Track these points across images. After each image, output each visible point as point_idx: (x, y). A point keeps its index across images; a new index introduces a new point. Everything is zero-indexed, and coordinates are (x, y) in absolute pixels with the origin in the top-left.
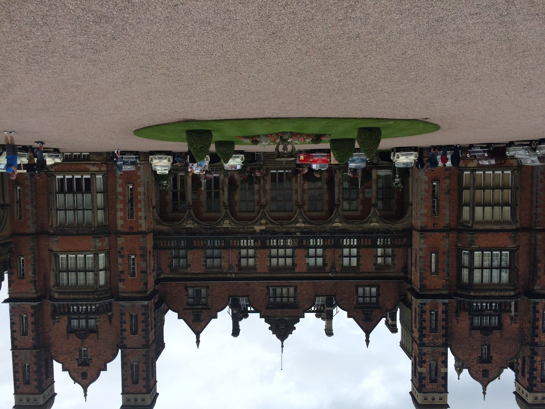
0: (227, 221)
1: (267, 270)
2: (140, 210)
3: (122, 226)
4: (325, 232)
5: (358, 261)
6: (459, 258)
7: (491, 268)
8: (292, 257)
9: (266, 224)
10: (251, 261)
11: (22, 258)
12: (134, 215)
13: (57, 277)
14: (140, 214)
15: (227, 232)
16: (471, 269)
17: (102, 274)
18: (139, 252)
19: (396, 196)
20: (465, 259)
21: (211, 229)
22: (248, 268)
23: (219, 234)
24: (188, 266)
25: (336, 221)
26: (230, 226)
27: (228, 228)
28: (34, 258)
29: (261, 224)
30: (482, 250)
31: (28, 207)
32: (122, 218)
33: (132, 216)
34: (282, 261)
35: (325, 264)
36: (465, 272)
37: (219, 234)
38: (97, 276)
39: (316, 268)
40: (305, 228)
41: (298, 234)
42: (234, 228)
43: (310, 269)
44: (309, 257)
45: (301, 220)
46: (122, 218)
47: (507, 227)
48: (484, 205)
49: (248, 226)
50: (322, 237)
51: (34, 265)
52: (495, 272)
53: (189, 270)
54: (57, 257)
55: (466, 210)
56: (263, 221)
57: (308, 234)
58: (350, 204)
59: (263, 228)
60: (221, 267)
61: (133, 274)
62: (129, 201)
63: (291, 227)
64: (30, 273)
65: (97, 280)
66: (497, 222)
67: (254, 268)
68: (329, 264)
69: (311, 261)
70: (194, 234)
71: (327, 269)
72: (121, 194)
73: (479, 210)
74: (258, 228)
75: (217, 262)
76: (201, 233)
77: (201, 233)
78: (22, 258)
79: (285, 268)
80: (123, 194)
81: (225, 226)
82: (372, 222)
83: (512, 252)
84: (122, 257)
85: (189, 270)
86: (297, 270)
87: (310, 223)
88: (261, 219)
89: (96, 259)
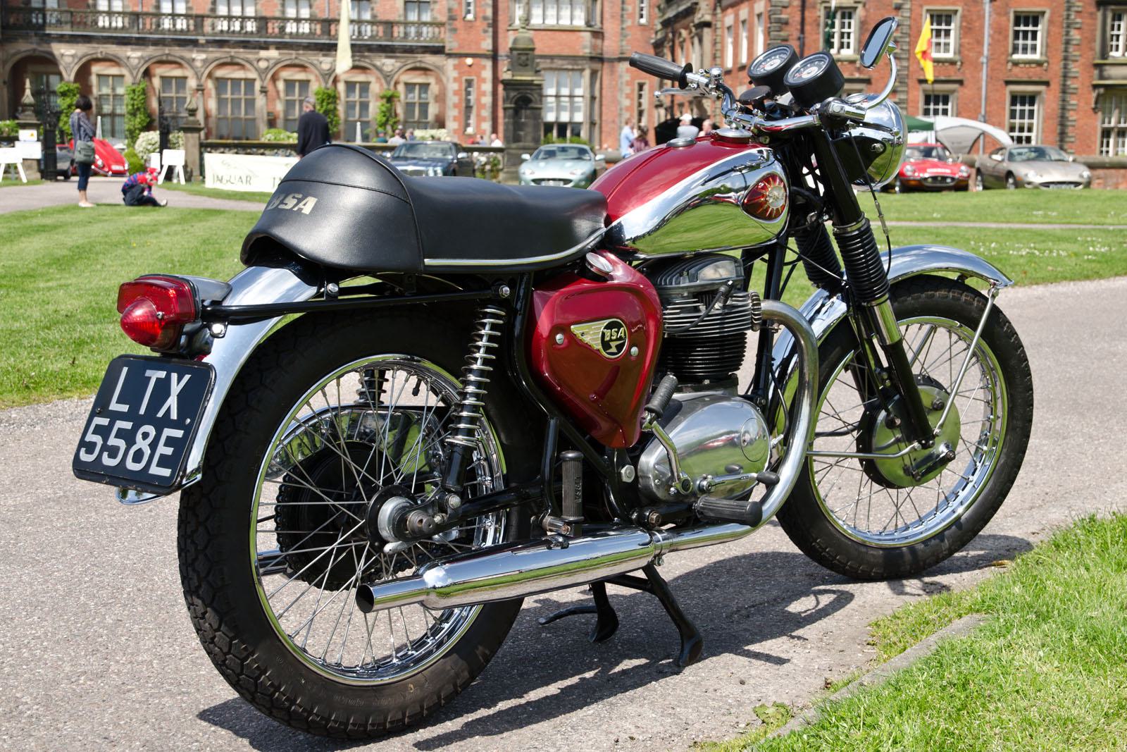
2: (456, 93)
3: (484, 67)
9: (259, 60)
11: (643, 21)
12: (464, 85)
14: (455, 86)
25: (136, 61)
26: (322, 59)
27: (324, 55)
28: (622, 22)
29: (267, 60)
31: (626, 103)
32: (484, 81)
33: (469, 83)
40: (191, 51)
42: (315, 55)
45: (198, 64)
46: (484, 81)
49: (288, 57)
50: (163, 32)
51: (623, 9)
54: (588, 24)
56: (263, 65)
59: (263, 54)
62: (471, 107)
72: (484, 119)
78: (643, 21)
80: (480, 119)
82: (73, 56)
84: (485, 18)
87: (182, 58)
88: (268, 69)
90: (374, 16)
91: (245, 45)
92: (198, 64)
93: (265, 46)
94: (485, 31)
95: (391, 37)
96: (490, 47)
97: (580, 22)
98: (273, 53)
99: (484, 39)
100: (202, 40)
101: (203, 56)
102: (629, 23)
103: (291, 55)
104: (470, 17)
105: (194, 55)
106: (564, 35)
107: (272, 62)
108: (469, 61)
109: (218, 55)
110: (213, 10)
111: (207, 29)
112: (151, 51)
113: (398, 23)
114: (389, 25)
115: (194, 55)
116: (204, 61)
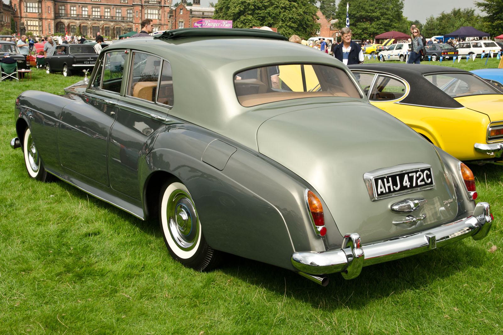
0: (112, 25)
1: (101, 7)
4: (82, 20)
5: (71, 8)
6: (42, 11)
7: (32, 7)
8: (93, 11)
10: (106, 10)
13: (158, 12)
16: (38, 7)
17: (146, 13)
18: (135, 18)
19: (59, 29)
20: (40, 10)
22: (108, 8)
23: (114, 21)
24: (127, 10)
30: (35, 13)
33: (137, 29)
34: (96, 10)
35: (82, 8)
36: (40, 6)
37: (114, 21)
38: (147, 12)
39: (85, 7)
41: (90, 19)
43: (86, 7)
44: (87, 11)
47: (29, 19)
48: (36, 26)
52: (31, 6)
53: (127, 9)
54: (158, 19)
55: (41, 25)
56: (101, 24)
57: (87, 19)
58: (74, 27)
59: (101, 22)
60: (116, 9)
61: (137, 12)
63: (92, 22)
64: (166, 14)
65: (147, 11)
66: (31, 20)
67: (105, 8)
68: (80, 8)
69: (86, 9)
70: (122, 22)
71: (81, 6)
73: (37, 24)
74: (102, 22)
75: (117, 11)
76: (120, 22)
77: (120, 22)
79: (95, 8)
81: (112, 23)
83: (27, 12)
85: (127, 9)
86: (91, 7)
88: (102, 25)
89: (147, 17)
91: (98, 20)
93: (101, 21)
97: (157, 18)
102: (166, 19)
105: (89, 22)
108: (137, 25)
110: (92, 14)
111: (91, 17)
112: (81, 21)
113: (125, 17)
114: (124, 17)
115: (89, 22)
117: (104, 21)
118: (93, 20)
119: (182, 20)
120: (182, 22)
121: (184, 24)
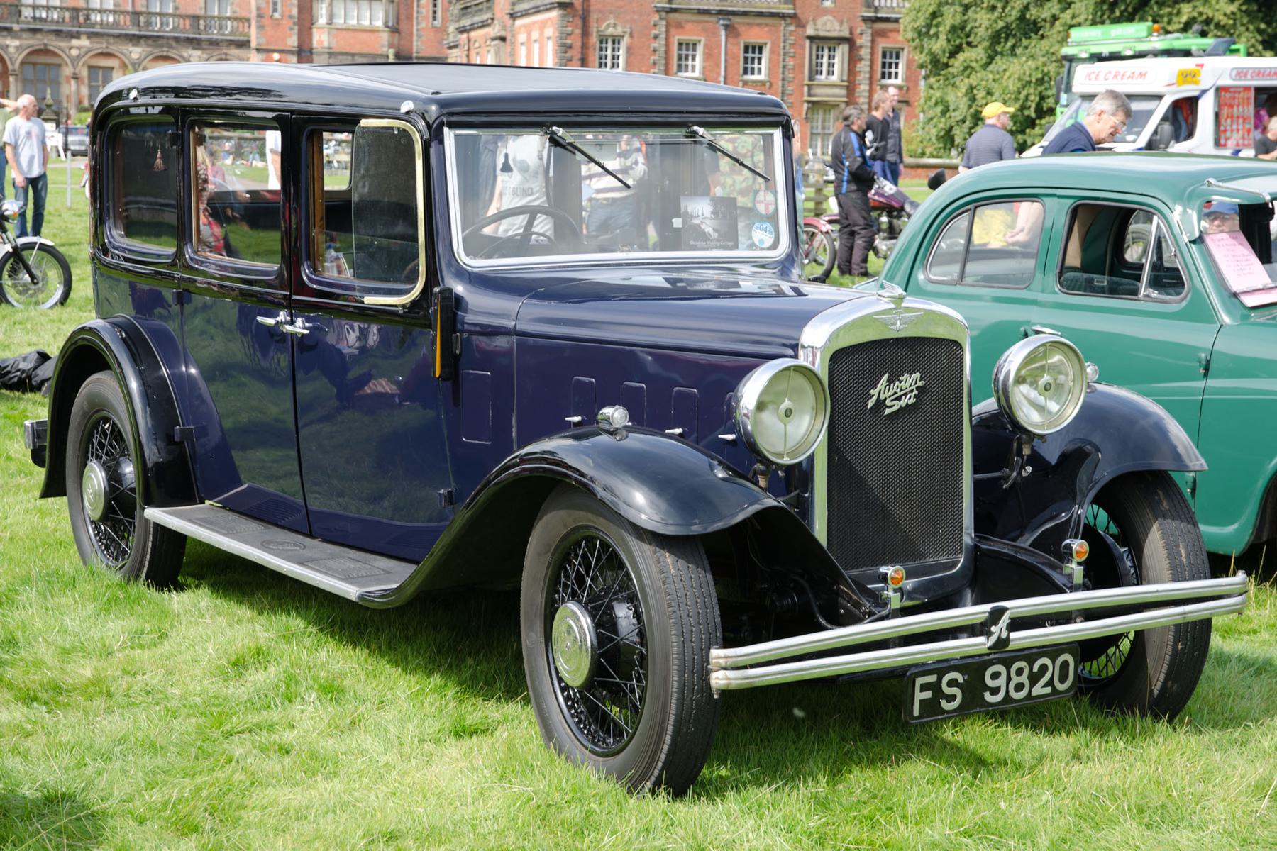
0: (134, 56)
15: (135, 39)
18: (266, 21)
21: (162, 46)
26: (131, 48)
29: (79, 48)
40: (4, 37)
56: (74, 52)
59: (75, 42)
76: (177, 39)
81: (138, 49)
84: (291, 17)
90: (176, 8)
91: (58, 33)
92: (12, 50)
93: (77, 36)
94: (291, 29)
95: (198, 31)
96: (296, 44)
97: (379, 23)
98: (84, 42)
99: (290, 36)
100: (16, 27)
101: (17, 43)
103: (102, 45)
104: (277, 15)
105: (8, 42)
106: (364, 35)
107: (83, 50)
109: (31, 42)
116: (17, 48)
117: (91, 36)
118: (34, 31)
119: (619, 31)
120: (616, 40)
121: (629, 49)
